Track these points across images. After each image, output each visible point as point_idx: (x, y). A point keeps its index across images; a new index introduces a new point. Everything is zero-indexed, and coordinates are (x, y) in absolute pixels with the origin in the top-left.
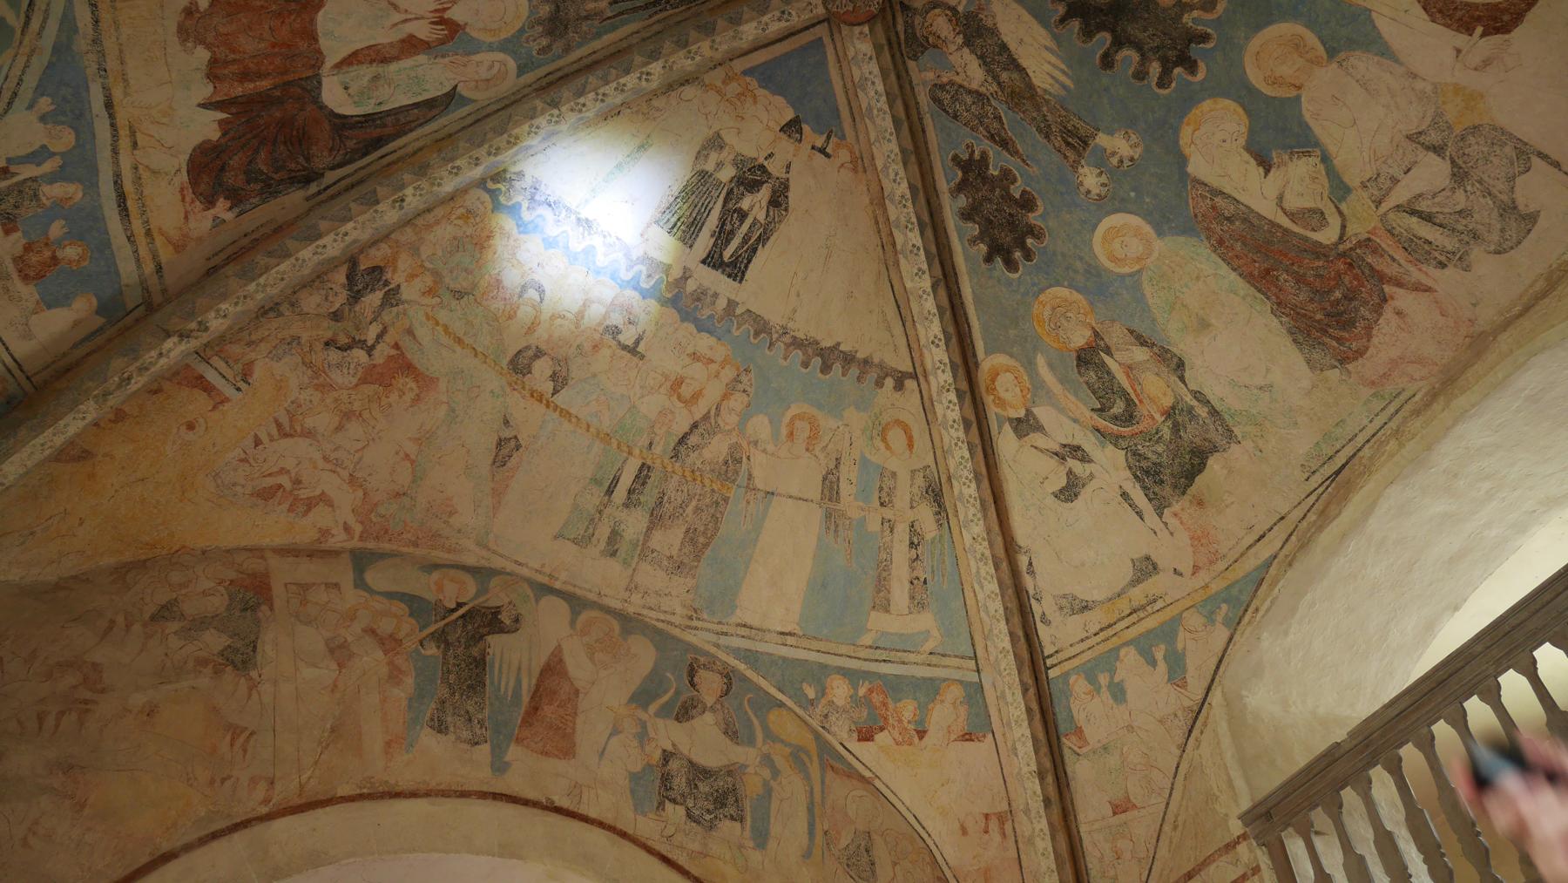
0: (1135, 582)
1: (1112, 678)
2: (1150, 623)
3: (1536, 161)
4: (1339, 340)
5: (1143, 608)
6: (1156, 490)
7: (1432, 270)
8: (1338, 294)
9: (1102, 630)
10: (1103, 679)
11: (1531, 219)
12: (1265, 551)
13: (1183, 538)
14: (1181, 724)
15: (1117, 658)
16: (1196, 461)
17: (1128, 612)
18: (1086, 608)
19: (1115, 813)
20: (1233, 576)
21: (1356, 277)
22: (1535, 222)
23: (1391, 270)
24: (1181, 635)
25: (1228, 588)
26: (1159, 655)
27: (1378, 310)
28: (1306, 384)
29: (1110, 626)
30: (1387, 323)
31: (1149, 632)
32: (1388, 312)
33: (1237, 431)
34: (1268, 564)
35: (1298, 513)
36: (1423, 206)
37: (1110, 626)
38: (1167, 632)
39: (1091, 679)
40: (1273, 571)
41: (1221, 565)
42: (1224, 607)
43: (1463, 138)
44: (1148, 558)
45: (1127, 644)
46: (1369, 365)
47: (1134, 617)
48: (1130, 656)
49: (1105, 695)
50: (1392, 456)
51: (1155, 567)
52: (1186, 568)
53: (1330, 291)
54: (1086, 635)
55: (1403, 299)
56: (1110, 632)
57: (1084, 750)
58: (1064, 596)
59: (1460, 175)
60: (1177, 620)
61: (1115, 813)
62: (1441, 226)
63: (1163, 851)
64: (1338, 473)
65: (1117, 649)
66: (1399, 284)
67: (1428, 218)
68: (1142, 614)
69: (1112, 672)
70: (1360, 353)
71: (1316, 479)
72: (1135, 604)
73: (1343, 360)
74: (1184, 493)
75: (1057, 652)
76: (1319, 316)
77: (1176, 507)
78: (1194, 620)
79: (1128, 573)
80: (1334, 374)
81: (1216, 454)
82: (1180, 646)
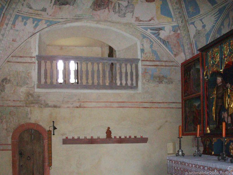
0: (41, 10)
1: (26, 21)
2: (38, 18)
3: (132, 14)
4: (96, 7)
5: (39, 15)
6: (57, 2)
7: (112, 11)
8: (103, 3)
9: (30, 13)
10: (25, 20)
11: (125, 17)
12: (61, 20)
13: (53, 10)
14: (31, 34)
15: (29, 19)
16: (66, 3)
17: (36, 13)
18: (31, 8)
19: (12, 41)
20: (54, 20)
21: (106, 4)
22: (124, 17)
23: (110, 7)
24: (40, 22)
25: (52, 21)
26: (35, 23)
27: (104, 9)
28: (88, 8)
29: (32, 14)
30: (103, 11)
31: (37, 19)
32: (104, 10)
33: (75, 5)
34: (59, 22)
35: (69, 19)
36: (120, 6)
37: (32, 14)
38: (39, 20)
39: (23, 19)
40: (59, 23)
41: (54, 18)
42: (49, 23)
43: (131, 4)
44: (46, 9)
45: (33, 18)
46: (95, 12)
47: (36, 15)
48: (31, 20)
49: (23, 23)
50: (84, 22)
51: (46, 11)
52: (50, 14)
53: (103, 2)
54: (27, 12)
55: (107, 10)
56: (31, 14)
57: (13, 29)
58: (29, 4)
59: (126, 7)
60: (41, 20)
61: (12, 41)
62: (119, 9)
63: (16, 50)
64: (78, 19)
65: (30, 18)
66: (108, 9)
67: (119, 6)
68: (38, 15)
69: (27, 20)
70: (96, 10)
71: (75, 18)
72: (38, 13)
73: (94, 9)
74: (59, 5)
75: (20, 11)
76: (98, 3)
77: (57, 6)
78: (44, 22)
79: (41, 8)
80: (91, 10)
81: (69, 5)
82: (39, 24)
